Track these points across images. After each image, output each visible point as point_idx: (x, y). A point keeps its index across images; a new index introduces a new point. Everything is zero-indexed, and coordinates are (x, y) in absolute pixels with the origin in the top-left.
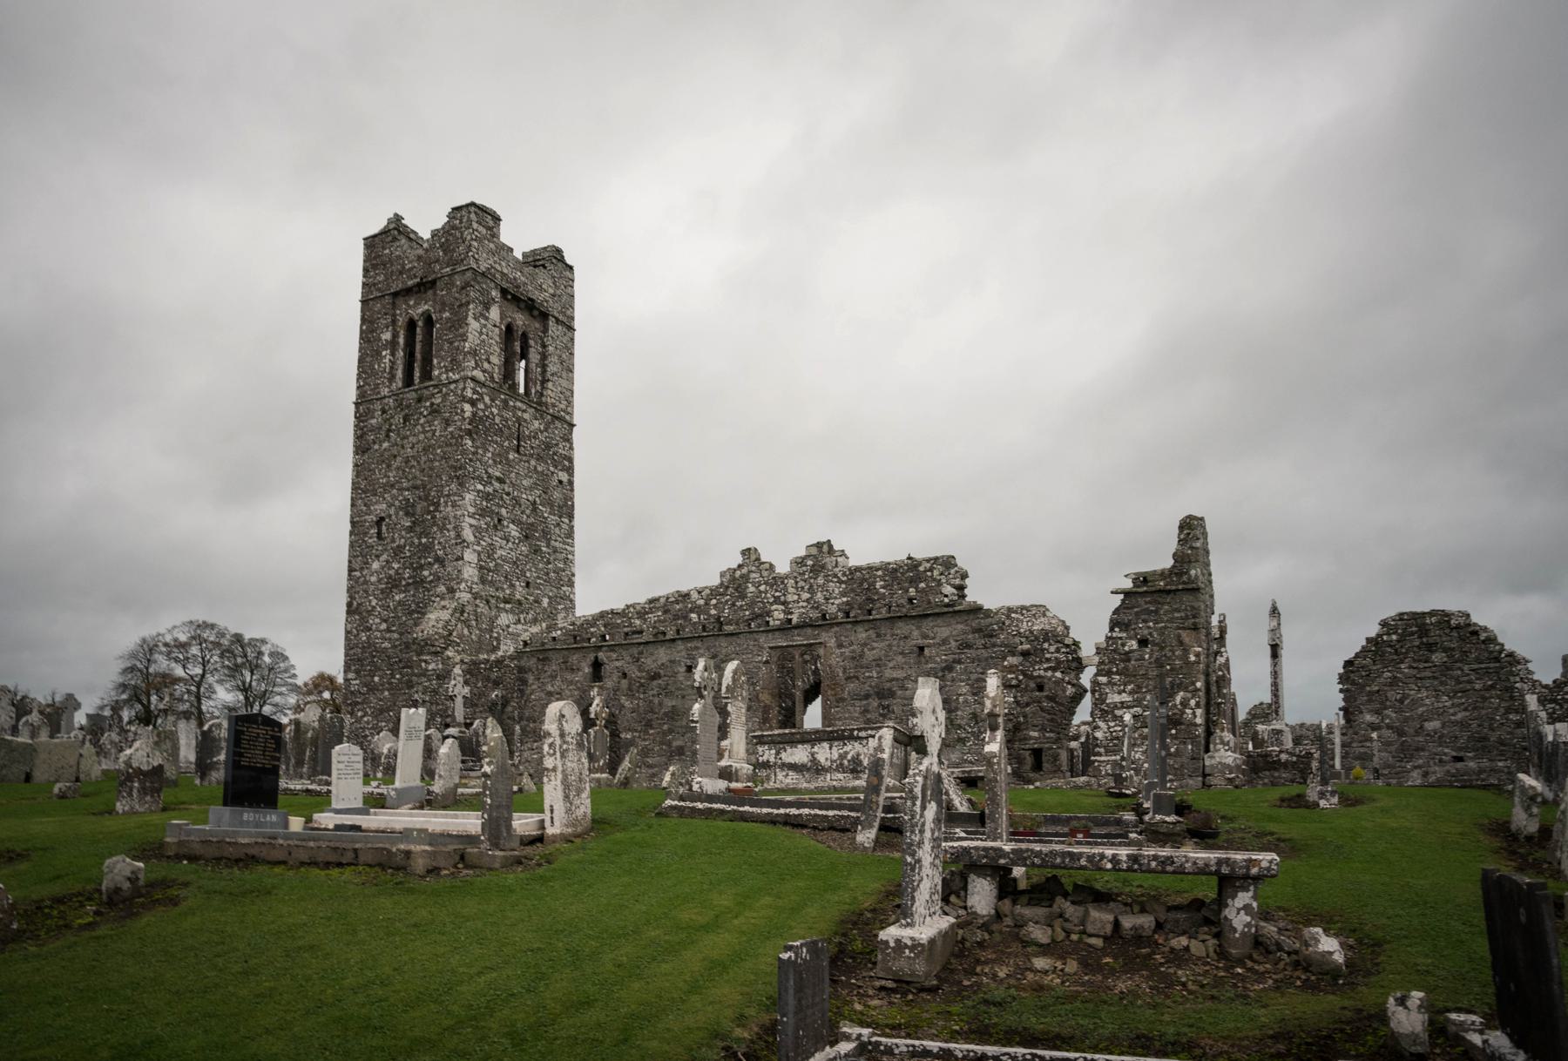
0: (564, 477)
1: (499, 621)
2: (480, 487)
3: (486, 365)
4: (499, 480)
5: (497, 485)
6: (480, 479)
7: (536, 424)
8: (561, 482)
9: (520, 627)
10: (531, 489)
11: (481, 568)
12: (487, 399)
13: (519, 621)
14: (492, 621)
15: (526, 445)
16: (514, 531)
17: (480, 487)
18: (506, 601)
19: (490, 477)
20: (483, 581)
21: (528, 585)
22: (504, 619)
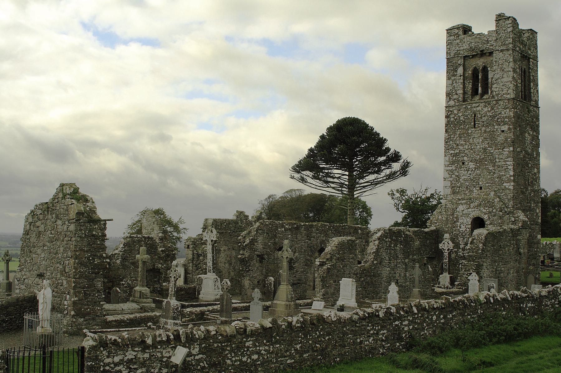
2: (453, 152)
3: (455, 97)
4: (462, 145)
5: (461, 148)
6: (452, 148)
7: (486, 109)
8: (503, 131)
9: (470, 210)
10: (483, 142)
12: (456, 112)
14: (454, 210)
15: (479, 123)
16: (472, 165)
17: (453, 152)
20: (454, 193)
21: (481, 188)
22: (461, 208)
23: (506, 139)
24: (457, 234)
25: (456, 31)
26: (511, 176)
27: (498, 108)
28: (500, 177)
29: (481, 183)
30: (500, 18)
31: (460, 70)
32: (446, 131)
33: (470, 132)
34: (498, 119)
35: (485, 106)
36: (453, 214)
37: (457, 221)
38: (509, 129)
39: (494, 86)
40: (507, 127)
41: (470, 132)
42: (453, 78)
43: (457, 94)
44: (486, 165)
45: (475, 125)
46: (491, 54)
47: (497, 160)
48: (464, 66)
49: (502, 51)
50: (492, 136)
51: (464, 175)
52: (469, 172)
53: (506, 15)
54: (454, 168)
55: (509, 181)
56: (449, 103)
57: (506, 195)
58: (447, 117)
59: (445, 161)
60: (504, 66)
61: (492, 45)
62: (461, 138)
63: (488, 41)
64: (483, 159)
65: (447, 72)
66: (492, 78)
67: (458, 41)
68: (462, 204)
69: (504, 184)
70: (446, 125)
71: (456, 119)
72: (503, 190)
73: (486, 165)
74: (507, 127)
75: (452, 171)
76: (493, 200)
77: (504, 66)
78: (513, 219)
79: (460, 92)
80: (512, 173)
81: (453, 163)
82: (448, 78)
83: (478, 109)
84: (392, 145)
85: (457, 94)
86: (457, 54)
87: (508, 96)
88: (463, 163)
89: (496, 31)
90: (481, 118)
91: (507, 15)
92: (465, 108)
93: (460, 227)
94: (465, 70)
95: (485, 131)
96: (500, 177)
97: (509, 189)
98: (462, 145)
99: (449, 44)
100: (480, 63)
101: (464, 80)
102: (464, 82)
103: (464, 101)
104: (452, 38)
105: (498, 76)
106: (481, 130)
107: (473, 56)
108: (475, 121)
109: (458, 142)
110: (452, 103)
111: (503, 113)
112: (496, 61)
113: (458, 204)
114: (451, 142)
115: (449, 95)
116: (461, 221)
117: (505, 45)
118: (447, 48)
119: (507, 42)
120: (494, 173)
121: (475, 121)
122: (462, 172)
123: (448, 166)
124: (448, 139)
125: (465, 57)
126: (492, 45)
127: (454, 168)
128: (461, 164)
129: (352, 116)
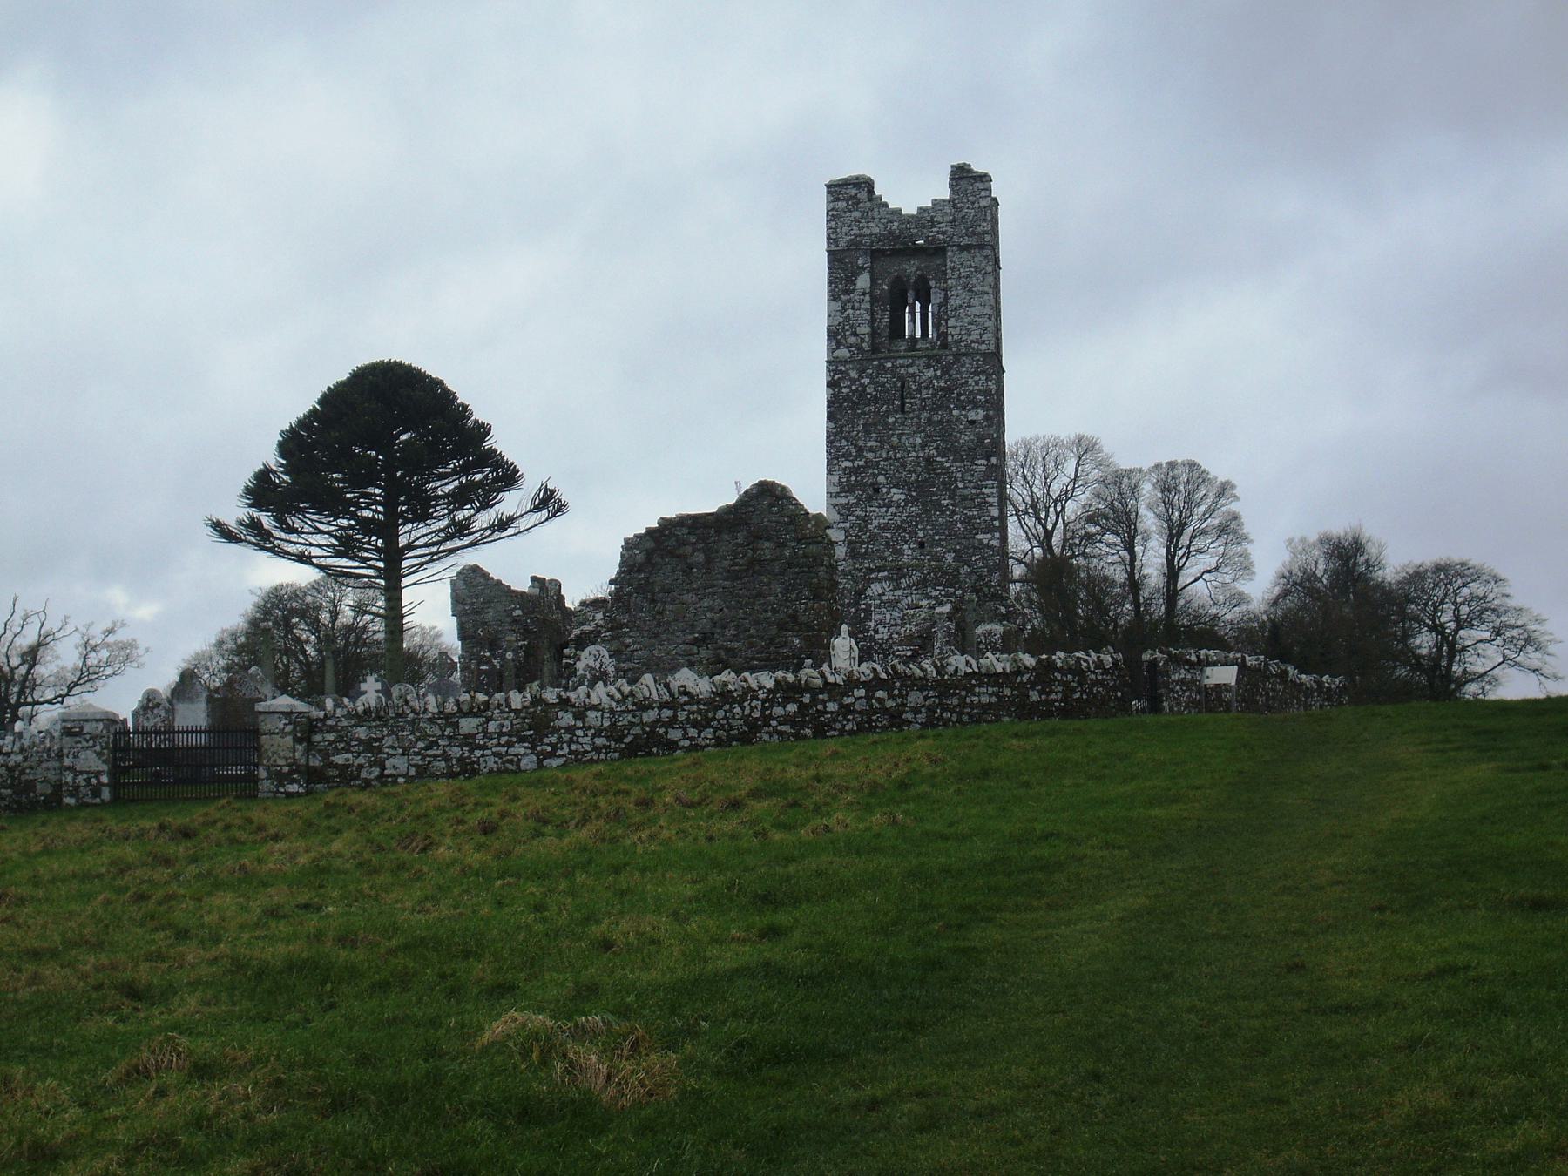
0: (979, 415)
1: (869, 592)
2: (848, 464)
3: (852, 340)
5: (870, 455)
6: (847, 456)
7: (930, 373)
8: (972, 422)
9: (900, 592)
10: (923, 446)
11: (850, 543)
12: (854, 374)
13: (898, 587)
14: (860, 593)
16: (897, 495)
17: (848, 464)
18: (879, 570)
19: (860, 450)
21: (922, 545)
22: (876, 588)
23: (981, 439)
24: (870, 648)
25: (854, 191)
26: (993, 519)
27: (959, 372)
28: (967, 521)
29: (921, 534)
30: (962, 176)
31: (863, 282)
32: (830, 417)
33: (891, 420)
34: (959, 395)
35: (928, 366)
36: (857, 604)
37: (868, 618)
38: (987, 417)
39: (951, 323)
40: (981, 413)
41: (891, 420)
42: (844, 297)
43: (855, 334)
44: (933, 494)
45: (903, 405)
46: (937, 250)
47: (961, 485)
48: (872, 273)
49: (967, 248)
50: (946, 430)
51: (879, 517)
52: (892, 510)
53: (975, 168)
54: (852, 500)
55: (990, 529)
56: (836, 353)
57: (983, 558)
58: (829, 385)
59: (830, 484)
60: (974, 281)
61: (943, 233)
62: (867, 433)
63: (932, 220)
64: (926, 480)
65: (830, 283)
66: (940, 305)
67: (857, 214)
68: (880, 581)
69: (980, 536)
70: (830, 403)
71: (854, 392)
72: (975, 548)
73: (933, 494)
74: (981, 413)
75: (847, 507)
76: (957, 570)
77: (974, 281)
78: (1003, 610)
79: (864, 329)
80: (995, 513)
81: (847, 489)
82: (834, 297)
83: (911, 370)
84: (501, 441)
85: (855, 334)
86: (855, 244)
87: (983, 347)
88: (877, 491)
89: (952, 202)
90: (919, 391)
91: (978, 167)
92: (878, 367)
93: (876, 632)
94: (873, 281)
95: (929, 419)
96: (967, 521)
97: (988, 546)
98: (871, 450)
99: (833, 218)
100: (911, 268)
101: (872, 303)
102: (872, 311)
103: (875, 349)
104: (841, 205)
105: (959, 302)
106: (918, 417)
107: (895, 253)
108: (902, 398)
109: (861, 443)
110: (843, 353)
111: (971, 382)
112: (953, 269)
113: (870, 581)
114: (844, 443)
115: (834, 335)
116: (879, 617)
117: (973, 233)
118: (829, 228)
119: (979, 229)
120: (954, 512)
121: (902, 398)
122: (873, 510)
123: (837, 495)
124: (836, 434)
125: (875, 254)
126: (943, 233)
127: (852, 500)
128: (870, 491)
129: (396, 357)
